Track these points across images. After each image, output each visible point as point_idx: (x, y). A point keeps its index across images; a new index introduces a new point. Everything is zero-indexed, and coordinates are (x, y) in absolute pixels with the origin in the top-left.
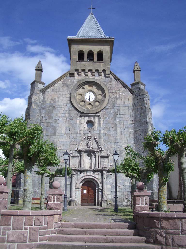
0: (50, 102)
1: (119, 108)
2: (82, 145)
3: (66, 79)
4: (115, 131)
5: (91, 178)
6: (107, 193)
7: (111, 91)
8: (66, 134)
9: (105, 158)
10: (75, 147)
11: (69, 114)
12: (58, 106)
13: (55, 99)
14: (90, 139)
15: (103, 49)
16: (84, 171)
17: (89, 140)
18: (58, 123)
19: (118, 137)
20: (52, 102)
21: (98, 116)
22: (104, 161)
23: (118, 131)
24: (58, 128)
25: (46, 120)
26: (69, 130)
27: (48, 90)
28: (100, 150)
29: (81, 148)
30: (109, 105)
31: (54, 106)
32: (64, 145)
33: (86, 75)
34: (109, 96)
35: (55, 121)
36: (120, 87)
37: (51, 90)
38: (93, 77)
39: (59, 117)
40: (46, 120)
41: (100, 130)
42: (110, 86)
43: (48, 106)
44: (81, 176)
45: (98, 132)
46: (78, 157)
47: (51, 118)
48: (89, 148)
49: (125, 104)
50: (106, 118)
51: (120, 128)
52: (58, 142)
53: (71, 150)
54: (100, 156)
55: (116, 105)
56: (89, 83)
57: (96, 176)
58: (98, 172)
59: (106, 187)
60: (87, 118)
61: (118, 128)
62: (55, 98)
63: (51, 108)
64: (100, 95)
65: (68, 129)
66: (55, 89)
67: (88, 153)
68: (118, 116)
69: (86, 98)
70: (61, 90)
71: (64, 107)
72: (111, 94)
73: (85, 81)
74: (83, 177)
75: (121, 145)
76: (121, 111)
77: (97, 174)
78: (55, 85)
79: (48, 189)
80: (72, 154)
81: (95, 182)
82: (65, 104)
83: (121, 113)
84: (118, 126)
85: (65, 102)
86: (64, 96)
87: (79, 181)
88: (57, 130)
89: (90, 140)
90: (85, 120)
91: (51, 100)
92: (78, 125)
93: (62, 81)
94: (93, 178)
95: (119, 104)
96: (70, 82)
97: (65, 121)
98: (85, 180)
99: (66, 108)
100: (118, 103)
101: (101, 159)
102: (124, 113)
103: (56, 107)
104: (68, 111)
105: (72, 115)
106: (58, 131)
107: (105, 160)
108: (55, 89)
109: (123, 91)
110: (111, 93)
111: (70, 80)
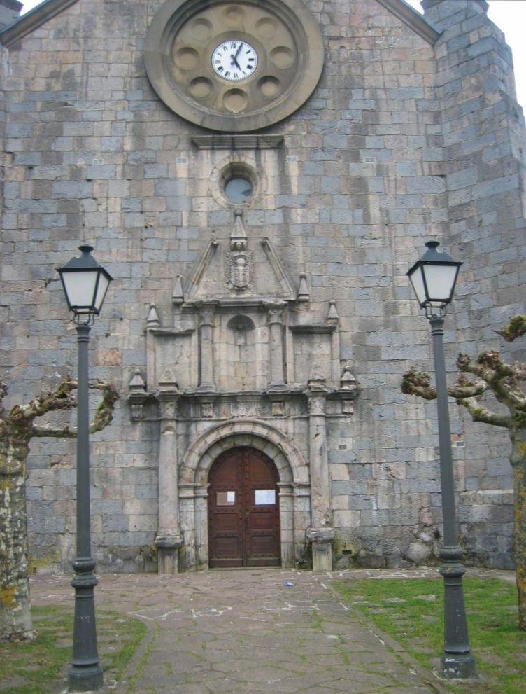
0: (49, 87)
1: (371, 105)
2: (204, 279)
4: (360, 212)
5: (252, 436)
6: (331, 504)
7: (332, 31)
8: (130, 231)
9: (317, 339)
10: (171, 289)
11: (139, 136)
12: (88, 105)
13: (71, 73)
14: (243, 248)
16: (217, 400)
17: (236, 254)
18: (89, 180)
19: (375, 238)
20: (57, 87)
21: (279, 146)
22: (314, 352)
23: (372, 212)
24: (88, 205)
25: (31, 168)
26: (142, 212)
27: (38, 33)
28: (290, 301)
29: (200, 294)
30: (324, 93)
31: (66, 104)
34: (326, 55)
35: (76, 174)
36: (375, 12)
37: (52, 33)
39: (93, 152)
40: (31, 168)
41: (285, 209)
42: (328, 8)
43: (39, 105)
44: (207, 425)
45: (278, 218)
46: (188, 334)
47: (51, 157)
48: (239, 290)
49: (399, 86)
50: (314, 150)
51: (382, 194)
53: (153, 304)
54: (290, 328)
55: (356, 93)
57: (278, 424)
58: (287, 406)
59: (326, 474)
60: (227, 153)
61: (371, 197)
62: (70, 67)
63: (50, 116)
65: (137, 207)
66: (72, 26)
67: (231, 316)
68: (370, 141)
69: (216, 66)
70: (99, 32)
71: (113, 108)
72: (334, 45)
74: (212, 430)
75: (389, 274)
76: (384, 118)
77: (280, 412)
78: (70, 11)
79: (45, 497)
80: (156, 324)
81: (271, 454)
82: (120, 95)
83: (381, 130)
84: (373, 185)
85: (118, 84)
86: (111, 58)
87: (197, 451)
88: (84, 212)
89: (242, 253)
90: (213, 163)
91: (54, 75)
92: (183, 190)
94: (263, 432)
95: (374, 90)
97: (119, 169)
98: (226, 446)
99: (124, 109)
100: (367, 84)
102: (397, 127)
103: (78, 107)
104: (131, 125)
105: (154, 143)
106: (89, 220)
107: (315, 346)
108: (72, 26)
109: (386, 30)
110: (331, 38)
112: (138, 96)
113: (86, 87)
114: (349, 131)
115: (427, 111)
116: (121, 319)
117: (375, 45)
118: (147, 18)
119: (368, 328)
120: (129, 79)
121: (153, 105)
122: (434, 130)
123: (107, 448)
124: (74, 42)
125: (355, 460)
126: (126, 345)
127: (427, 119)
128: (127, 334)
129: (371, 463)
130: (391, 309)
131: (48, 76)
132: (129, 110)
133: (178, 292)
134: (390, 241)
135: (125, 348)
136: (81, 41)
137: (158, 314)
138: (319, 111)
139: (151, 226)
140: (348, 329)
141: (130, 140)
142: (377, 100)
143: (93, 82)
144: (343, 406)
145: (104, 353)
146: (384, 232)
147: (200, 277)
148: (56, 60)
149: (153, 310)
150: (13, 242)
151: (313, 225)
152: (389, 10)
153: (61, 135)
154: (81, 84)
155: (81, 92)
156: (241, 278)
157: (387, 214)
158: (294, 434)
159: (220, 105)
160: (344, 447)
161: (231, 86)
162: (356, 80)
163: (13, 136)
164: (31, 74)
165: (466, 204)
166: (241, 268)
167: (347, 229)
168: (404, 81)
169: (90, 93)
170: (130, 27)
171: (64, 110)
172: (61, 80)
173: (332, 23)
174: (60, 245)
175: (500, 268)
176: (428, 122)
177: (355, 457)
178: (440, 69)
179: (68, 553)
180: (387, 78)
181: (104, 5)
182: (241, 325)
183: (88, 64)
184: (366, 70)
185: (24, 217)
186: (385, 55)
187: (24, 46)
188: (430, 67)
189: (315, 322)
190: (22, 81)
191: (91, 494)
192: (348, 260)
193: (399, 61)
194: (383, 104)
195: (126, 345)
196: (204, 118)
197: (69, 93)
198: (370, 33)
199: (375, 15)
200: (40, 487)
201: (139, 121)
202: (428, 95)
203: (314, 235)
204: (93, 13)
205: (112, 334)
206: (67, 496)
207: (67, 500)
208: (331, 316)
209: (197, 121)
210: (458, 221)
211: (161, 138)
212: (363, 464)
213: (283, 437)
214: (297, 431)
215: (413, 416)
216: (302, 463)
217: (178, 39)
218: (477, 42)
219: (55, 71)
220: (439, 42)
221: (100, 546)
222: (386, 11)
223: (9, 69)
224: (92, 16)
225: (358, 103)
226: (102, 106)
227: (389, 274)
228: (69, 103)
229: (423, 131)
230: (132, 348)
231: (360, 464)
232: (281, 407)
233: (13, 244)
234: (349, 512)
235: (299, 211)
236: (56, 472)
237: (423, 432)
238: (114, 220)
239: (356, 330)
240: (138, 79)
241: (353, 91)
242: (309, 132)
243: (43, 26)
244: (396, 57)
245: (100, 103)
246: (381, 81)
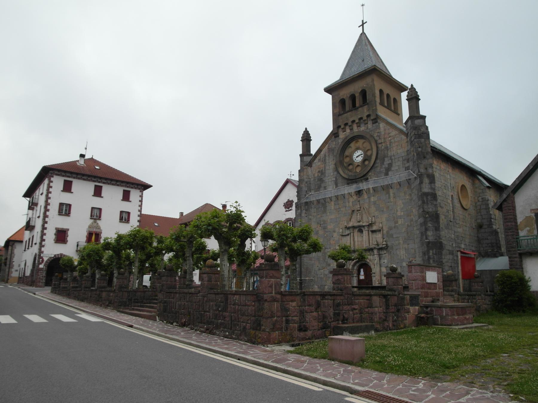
1: (390, 162)
2: (352, 220)
3: (331, 141)
4: (388, 195)
7: (379, 141)
9: (378, 233)
14: (359, 211)
27: (315, 161)
29: (351, 225)
30: (378, 161)
31: (321, 179)
42: (379, 134)
43: (316, 180)
46: (348, 235)
49: (398, 153)
55: (386, 159)
66: (322, 158)
73: (349, 138)
76: (394, 165)
82: (332, 174)
86: (330, 164)
89: (359, 212)
91: (319, 172)
93: (327, 146)
96: (335, 144)
100: (389, 155)
101: (372, 235)
112: (336, 173)
114: (384, 171)
117: (391, 142)
119: (390, 228)
127: (405, 162)
130: (396, 222)
133: (346, 224)
137: (342, 230)
138: (377, 167)
140: (385, 230)
142: (392, 160)
144: (384, 251)
147: (351, 219)
149: (341, 229)
151: (376, 201)
156: (359, 219)
159: (355, 170)
161: (357, 164)
166: (359, 216)
168: (399, 151)
171: (321, 180)
173: (380, 139)
182: (361, 231)
185: (315, 209)
186: (394, 145)
187: (313, 166)
192: (385, 210)
193: (397, 145)
196: (349, 177)
198: (390, 139)
201: (336, 180)
202: (406, 154)
208: (380, 226)
209: (347, 177)
213: (370, 260)
215: (402, 253)
217: (345, 154)
225: (387, 161)
226: (328, 178)
227: (395, 212)
232: (369, 252)
235: (373, 197)
237: (405, 258)
238: (333, 208)
239: (387, 229)
242: (374, 174)
244: (397, 144)
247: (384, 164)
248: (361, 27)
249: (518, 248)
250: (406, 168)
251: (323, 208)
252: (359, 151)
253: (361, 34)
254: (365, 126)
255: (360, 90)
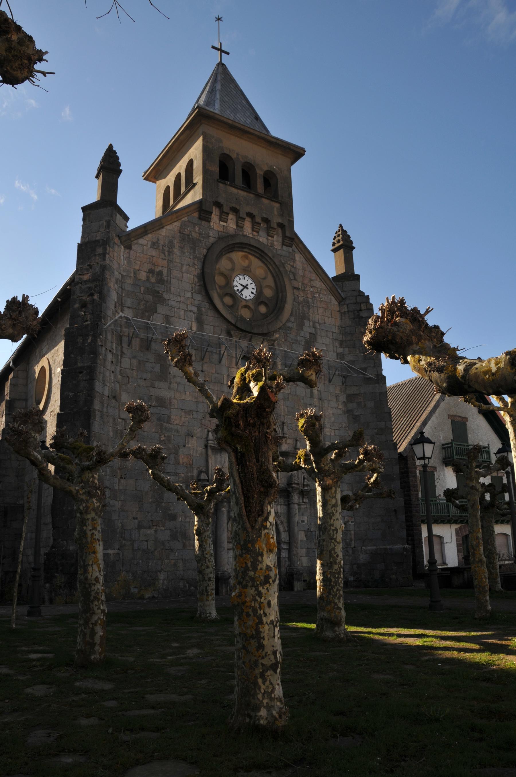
0: (148, 279)
1: (312, 330)
13: (160, 273)
15: (277, 169)
27: (141, 241)
32: (189, 412)
33: (237, 226)
37: (150, 244)
38: (253, 235)
49: (325, 323)
52: (174, 402)
55: (306, 323)
56: (245, 248)
62: (160, 268)
64: (269, 287)
73: (238, 242)
76: (319, 339)
79: (149, 548)
86: (184, 268)
91: (151, 271)
95: (314, 322)
99: (191, 304)
100: (311, 318)
103: (166, 296)
104: (196, 315)
108: (161, 242)
111: (199, 229)
112: (198, 297)
113: (170, 285)
114: (303, 343)
115: (337, 340)
116: (192, 437)
117: (314, 297)
118: (203, 249)
120: (194, 285)
121: (207, 305)
122: (340, 350)
123: (186, 518)
124: (162, 253)
125: (309, 529)
126: (195, 453)
127: (337, 344)
128: (195, 446)
129: (315, 531)
131: (148, 271)
132: (194, 305)
134: (322, 409)
135: (195, 455)
136: (167, 253)
139: (207, 381)
141: (196, 325)
142: (315, 328)
143: (173, 281)
145: (183, 457)
146: (319, 404)
148: (152, 262)
150: (128, 377)
152: (320, 279)
153: (156, 312)
154: (167, 281)
155: (167, 287)
157: (321, 393)
158: (281, 513)
160: (303, 521)
161: (244, 303)
162: (306, 315)
163: (127, 305)
164: (137, 267)
165: (356, 394)
167: (303, 399)
169: (172, 289)
170: (194, 253)
172: (155, 276)
174: (157, 384)
175: (376, 431)
176: (337, 346)
177: (308, 528)
178: (343, 318)
179: (163, 584)
180: (320, 317)
181: (179, 234)
183: (171, 270)
184: (310, 310)
185: (135, 362)
188: (338, 316)
189: (290, 450)
190: (132, 270)
191: (433, 531)
194: (318, 331)
195: (195, 453)
197: (160, 285)
198: (312, 289)
199: (314, 280)
200: (146, 541)
203: (288, 400)
204: (173, 237)
205: (187, 446)
206: (162, 547)
207: (162, 549)
209: (233, 322)
210: (352, 402)
211: (213, 327)
212: (312, 531)
214: (282, 512)
216: (285, 530)
218: (365, 310)
219: (151, 269)
220: (343, 303)
221: (182, 579)
222: (318, 279)
223: (124, 261)
224: (172, 239)
225: (307, 329)
228: (160, 292)
229: (335, 350)
230: (198, 455)
231: (311, 531)
233: (128, 378)
234: (306, 558)
236: (156, 531)
240: (199, 287)
241: (305, 321)
242: (286, 340)
243: (144, 237)
245: (178, 297)
246: (317, 318)
247: (303, 331)
248: (223, 54)
249: (438, 513)
250: (337, 354)
251: (158, 365)
252: (247, 278)
253: (218, 64)
254: (268, 239)
255: (266, 168)
